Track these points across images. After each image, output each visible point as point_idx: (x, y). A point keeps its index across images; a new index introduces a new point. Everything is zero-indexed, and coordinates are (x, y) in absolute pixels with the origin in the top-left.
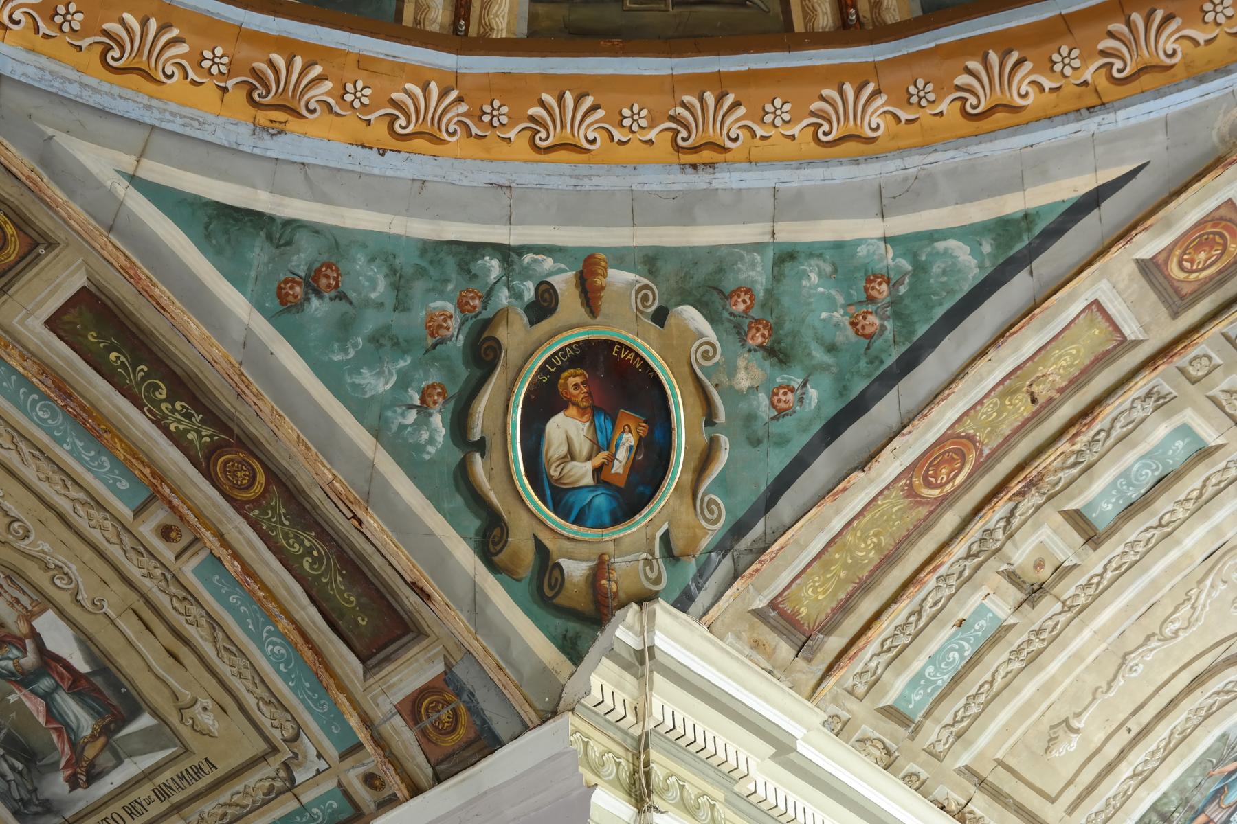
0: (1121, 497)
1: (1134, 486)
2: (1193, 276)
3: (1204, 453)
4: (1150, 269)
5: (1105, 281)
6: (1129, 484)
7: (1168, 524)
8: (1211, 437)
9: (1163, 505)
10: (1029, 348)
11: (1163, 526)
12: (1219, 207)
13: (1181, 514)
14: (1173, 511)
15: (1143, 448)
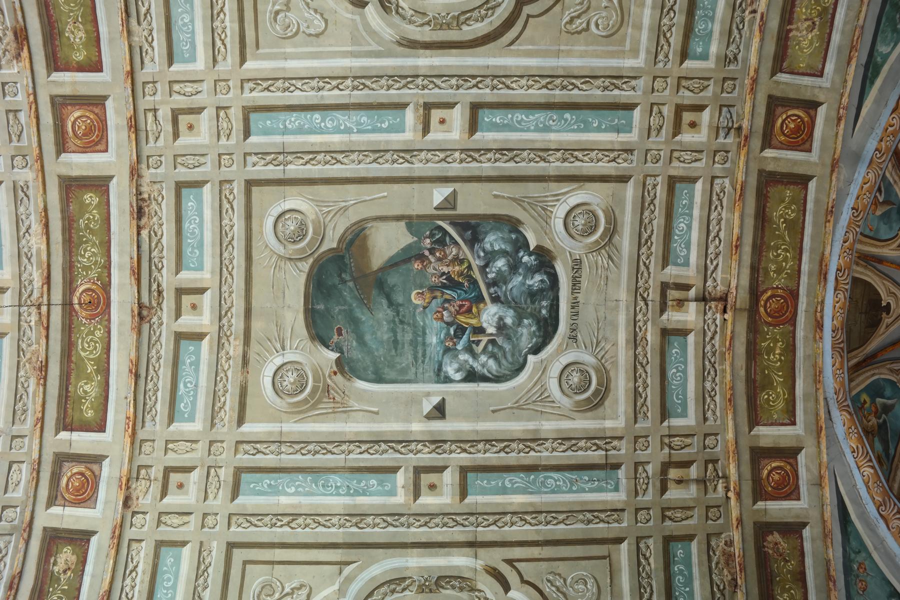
0: (704, 7)
1: (703, 16)
2: (784, 116)
3: (684, 55)
4: (812, 106)
5: (829, 86)
6: (706, 16)
7: (668, 12)
8: (688, 64)
9: (680, 19)
10: (836, 38)
11: (669, 10)
12: (811, 145)
13: (665, 21)
14: (671, 20)
15: (716, 35)
